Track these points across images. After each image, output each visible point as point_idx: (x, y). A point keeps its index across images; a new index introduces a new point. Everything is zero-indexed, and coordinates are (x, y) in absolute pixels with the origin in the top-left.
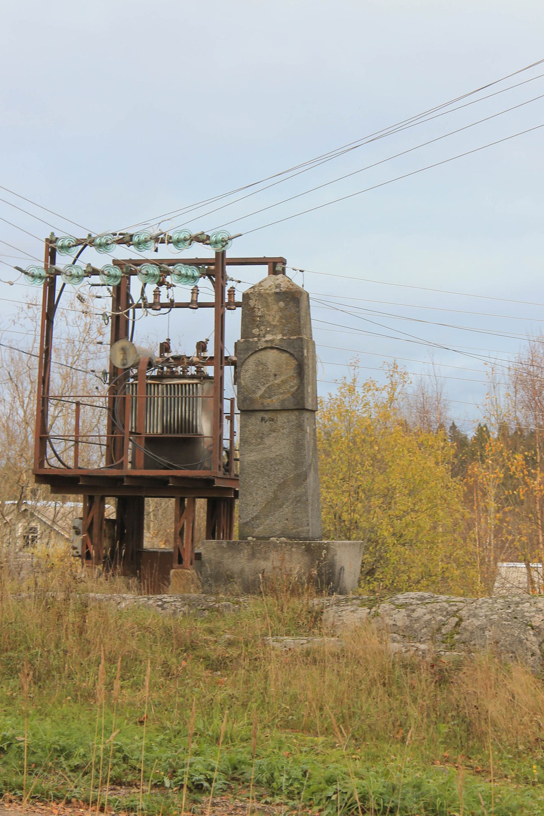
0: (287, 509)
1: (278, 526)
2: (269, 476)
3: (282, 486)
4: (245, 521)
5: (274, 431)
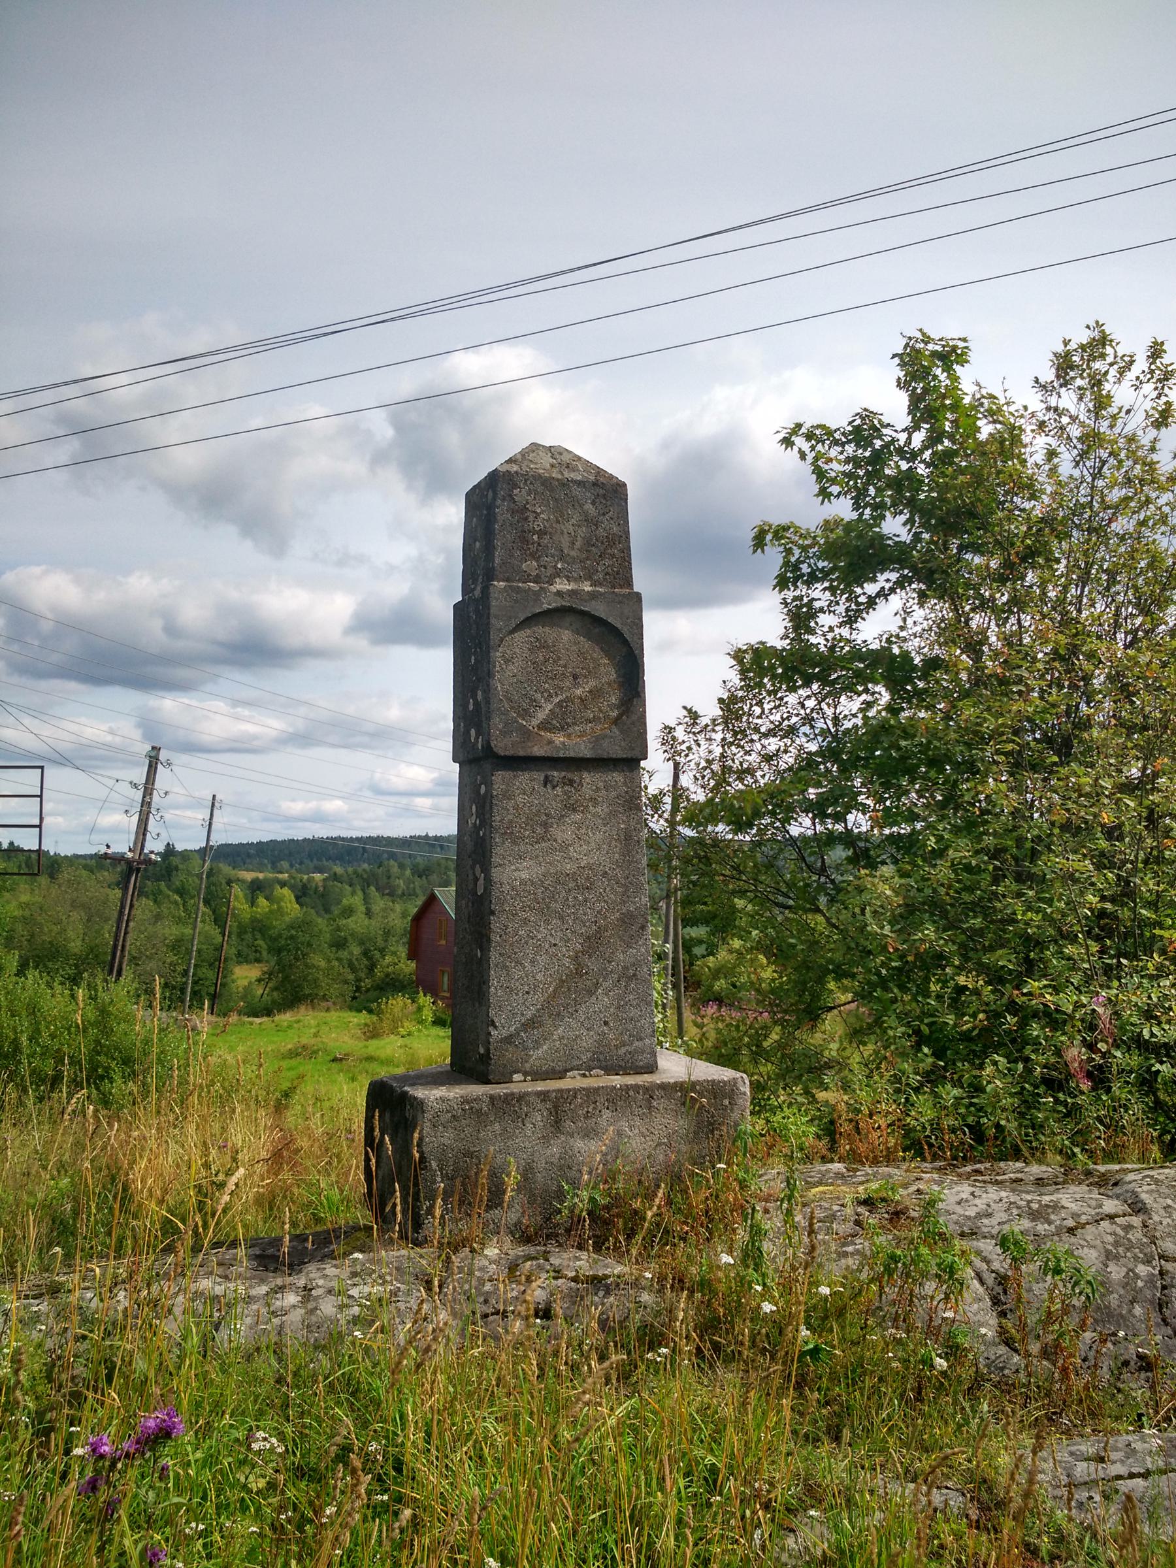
0: (602, 1001)
1: (588, 1041)
2: (561, 918)
3: (594, 942)
4: (505, 1033)
5: (574, 810)
